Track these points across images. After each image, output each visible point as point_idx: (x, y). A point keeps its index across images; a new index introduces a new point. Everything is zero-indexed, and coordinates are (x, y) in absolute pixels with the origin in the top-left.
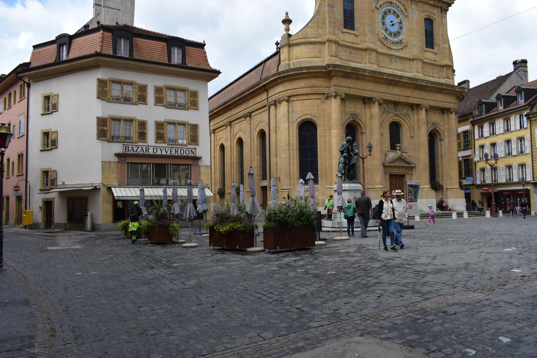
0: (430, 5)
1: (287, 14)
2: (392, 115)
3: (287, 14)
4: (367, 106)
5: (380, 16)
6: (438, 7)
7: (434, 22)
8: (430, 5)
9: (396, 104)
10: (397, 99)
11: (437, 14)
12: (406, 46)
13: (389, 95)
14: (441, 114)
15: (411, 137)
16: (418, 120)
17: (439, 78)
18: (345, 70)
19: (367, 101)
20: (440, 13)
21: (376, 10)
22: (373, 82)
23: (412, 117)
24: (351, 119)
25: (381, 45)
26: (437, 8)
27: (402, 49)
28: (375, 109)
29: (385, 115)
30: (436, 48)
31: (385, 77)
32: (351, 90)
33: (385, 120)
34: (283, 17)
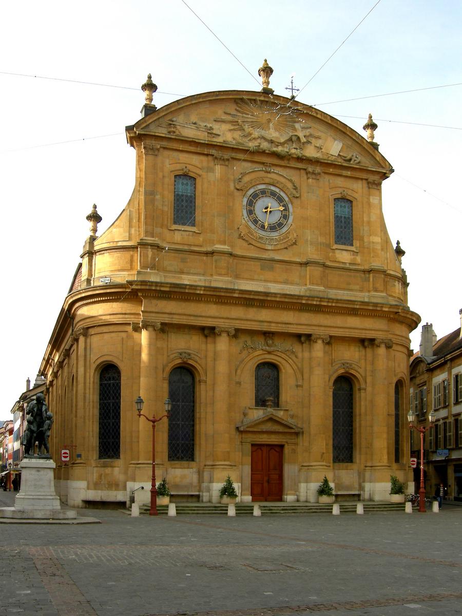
0: (346, 177)
1: (95, 207)
2: (261, 352)
3: (95, 207)
4: (210, 339)
5: (245, 200)
6: (362, 179)
7: (354, 203)
8: (346, 177)
9: (267, 335)
10: (265, 327)
11: (360, 190)
12: (295, 243)
13: (249, 323)
14: (361, 349)
15: (297, 386)
16: (310, 358)
17: (361, 291)
18: (158, 288)
19: (209, 332)
20: (366, 189)
21: (237, 193)
22: (216, 303)
23: (300, 355)
24: (179, 361)
25: (245, 244)
26: (360, 182)
27: (286, 248)
28: (223, 344)
29: (245, 352)
30: (356, 243)
31: (236, 295)
32: (175, 316)
33: (246, 360)
34: (89, 211)
